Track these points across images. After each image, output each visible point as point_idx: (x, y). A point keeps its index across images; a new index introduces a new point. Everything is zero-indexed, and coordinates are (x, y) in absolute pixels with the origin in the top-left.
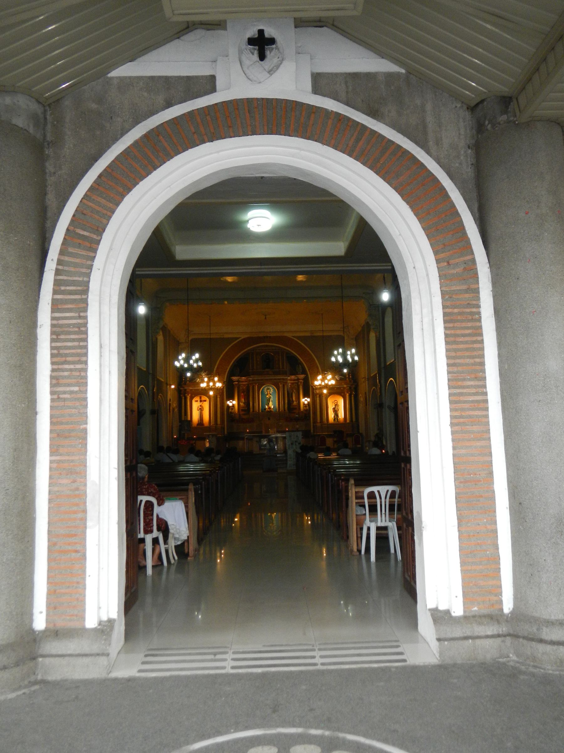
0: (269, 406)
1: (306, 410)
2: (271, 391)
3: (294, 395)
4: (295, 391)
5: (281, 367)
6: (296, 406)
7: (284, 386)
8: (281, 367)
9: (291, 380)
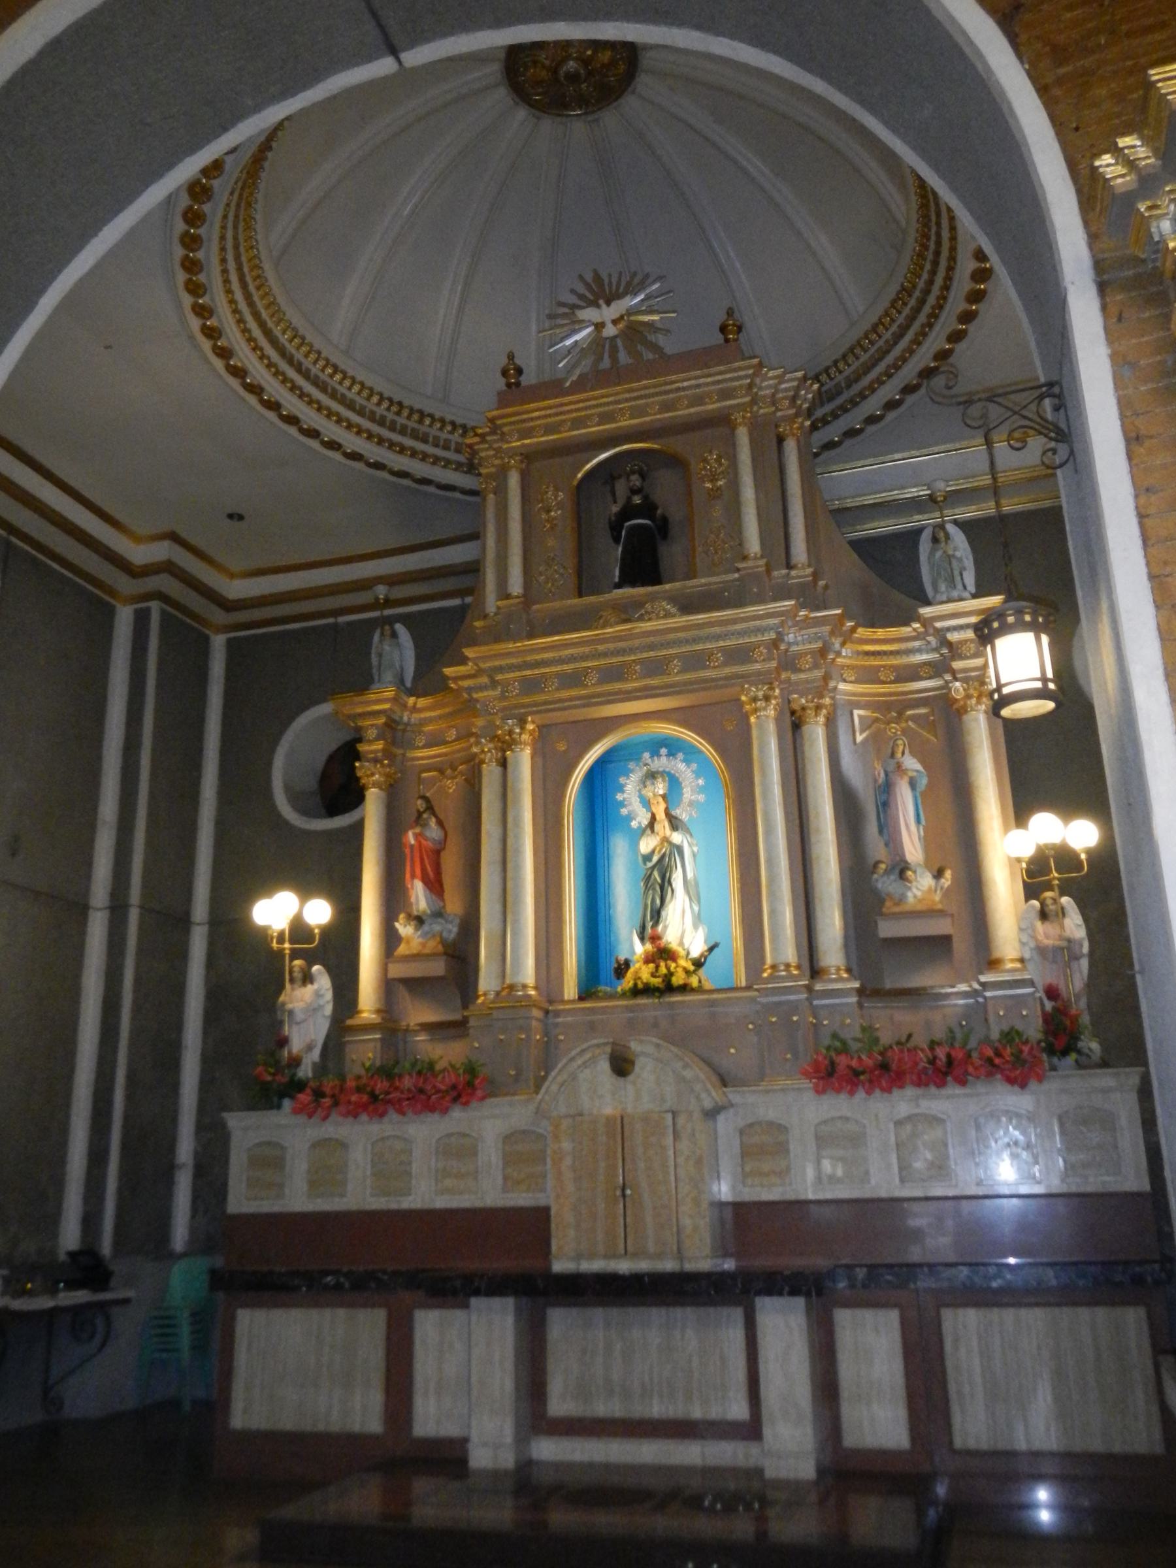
0: (655, 938)
1: (1064, 953)
2: (688, 794)
3: (906, 802)
4: (911, 764)
5: (753, 544)
6: (931, 913)
7: (794, 724)
8: (753, 544)
9: (869, 676)
